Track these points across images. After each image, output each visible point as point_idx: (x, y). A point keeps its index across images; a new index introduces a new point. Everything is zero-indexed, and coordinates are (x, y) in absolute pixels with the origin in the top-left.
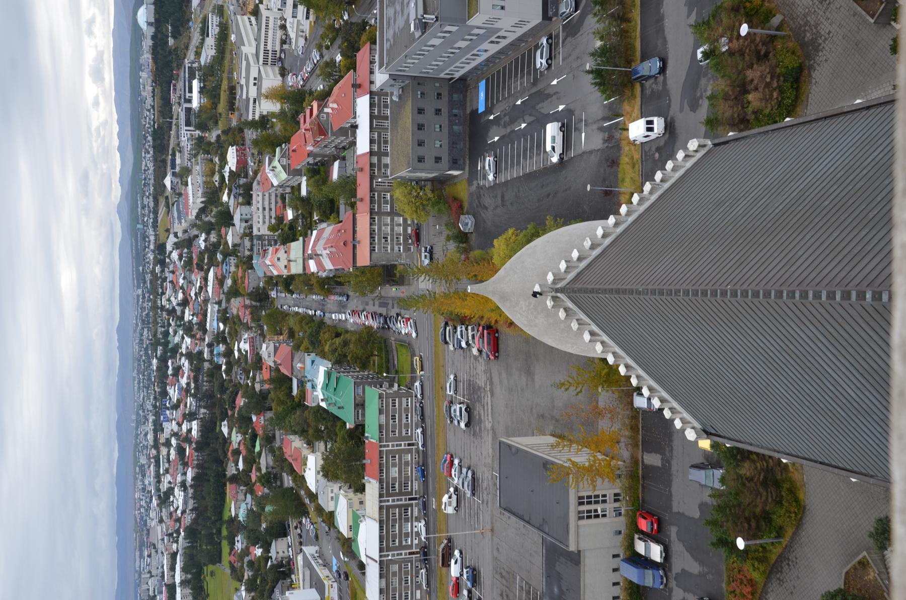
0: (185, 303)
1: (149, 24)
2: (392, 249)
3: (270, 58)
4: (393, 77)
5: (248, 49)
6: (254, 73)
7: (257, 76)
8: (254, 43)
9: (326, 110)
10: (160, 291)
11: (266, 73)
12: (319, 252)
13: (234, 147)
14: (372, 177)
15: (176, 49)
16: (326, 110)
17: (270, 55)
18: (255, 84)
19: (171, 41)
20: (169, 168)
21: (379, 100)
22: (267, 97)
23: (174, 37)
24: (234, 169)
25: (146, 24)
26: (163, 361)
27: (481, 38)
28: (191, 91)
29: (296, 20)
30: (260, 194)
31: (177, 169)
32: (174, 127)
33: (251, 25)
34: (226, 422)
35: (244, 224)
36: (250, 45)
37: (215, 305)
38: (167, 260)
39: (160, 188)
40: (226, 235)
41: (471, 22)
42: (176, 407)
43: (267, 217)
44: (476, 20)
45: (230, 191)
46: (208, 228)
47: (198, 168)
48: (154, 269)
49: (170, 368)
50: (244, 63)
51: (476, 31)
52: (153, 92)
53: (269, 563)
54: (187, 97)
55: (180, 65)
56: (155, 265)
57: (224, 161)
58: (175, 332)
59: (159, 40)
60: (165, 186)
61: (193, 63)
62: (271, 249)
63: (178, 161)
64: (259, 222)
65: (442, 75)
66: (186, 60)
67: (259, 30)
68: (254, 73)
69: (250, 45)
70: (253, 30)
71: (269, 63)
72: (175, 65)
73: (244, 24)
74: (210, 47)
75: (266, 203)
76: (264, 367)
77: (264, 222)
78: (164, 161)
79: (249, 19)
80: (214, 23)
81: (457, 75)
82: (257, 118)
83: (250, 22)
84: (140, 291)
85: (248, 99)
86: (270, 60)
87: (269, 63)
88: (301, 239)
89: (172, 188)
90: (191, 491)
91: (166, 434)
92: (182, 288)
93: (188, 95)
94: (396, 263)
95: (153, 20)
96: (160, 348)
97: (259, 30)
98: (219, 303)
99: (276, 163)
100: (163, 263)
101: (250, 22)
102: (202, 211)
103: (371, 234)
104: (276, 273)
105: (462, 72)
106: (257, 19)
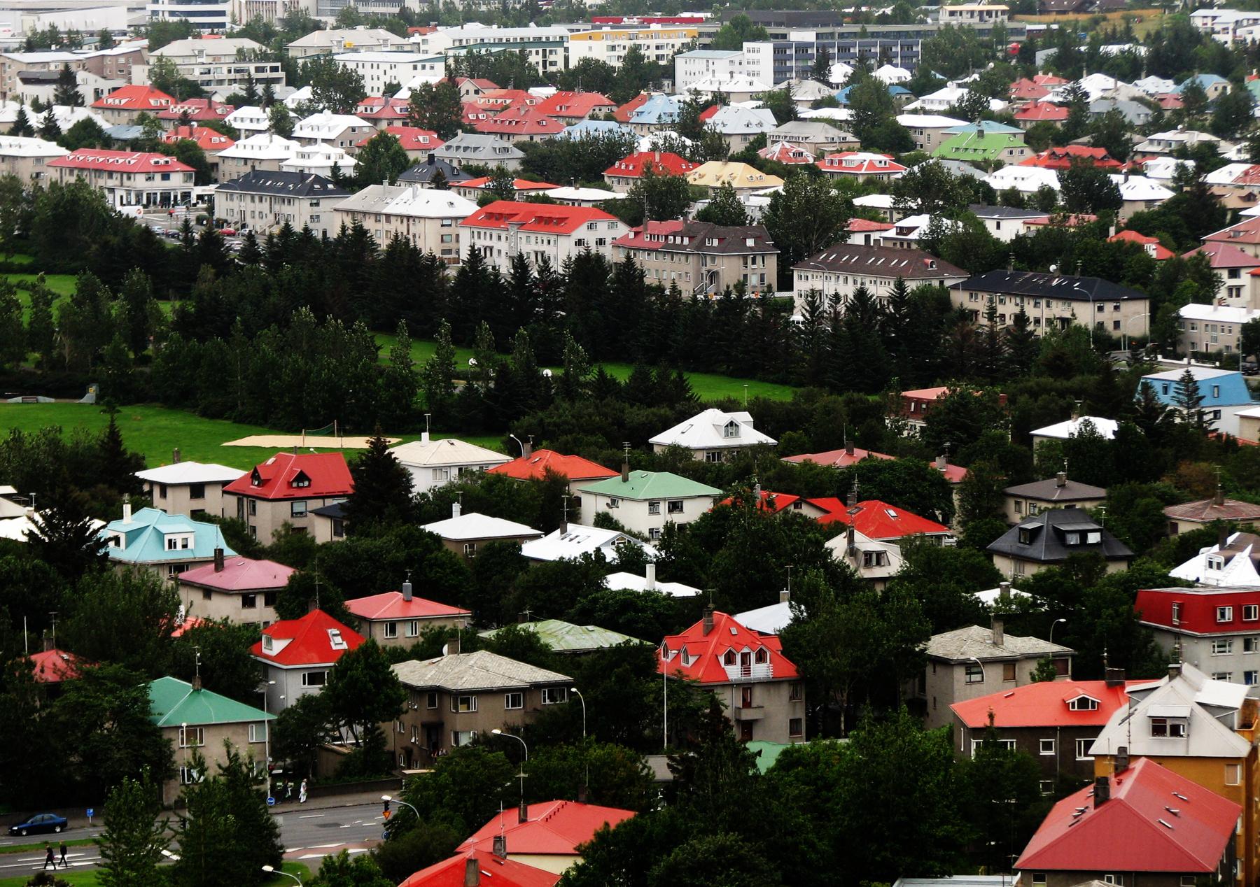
34: (750, 436)
76: (1091, 689)
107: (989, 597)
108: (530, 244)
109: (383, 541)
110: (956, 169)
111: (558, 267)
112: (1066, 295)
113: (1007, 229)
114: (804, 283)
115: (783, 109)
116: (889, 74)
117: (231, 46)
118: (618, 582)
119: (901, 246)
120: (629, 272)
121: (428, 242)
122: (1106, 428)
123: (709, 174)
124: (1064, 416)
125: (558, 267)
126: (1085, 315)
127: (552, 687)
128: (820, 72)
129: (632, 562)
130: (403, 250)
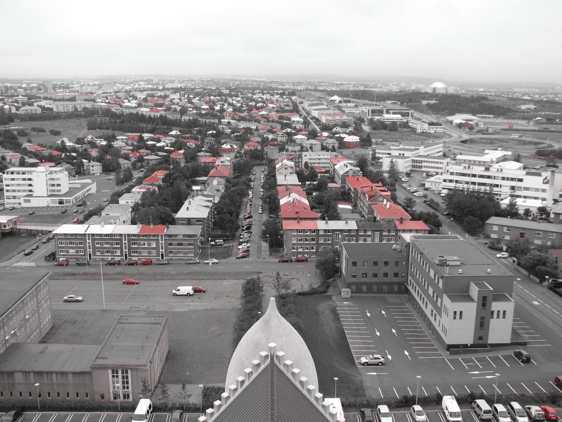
1: (434, 89)
2: (294, 244)
3: (417, 164)
4: (408, 245)
5: (422, 151)
6: (407, 154)
7: (405, 156)
8: (426, 154)
9: (385, 200)
10: (266, 92)
11: (406, 162)
12: (291, 195)
13: (359, 140)
14: (342, 231)
16: (385, 200)
17: (419, 164)
18: (400, 154)
19: (424, 102)
21: (392, 236)
22: (392, 162)
24: (345, 140)
25: (434, 87)
27: (434, 304)
28: (394, 113)
29: (442, 181)
30: (329, 157)
31: (344, 104)
32: (370, 102)
33: (437, 153)
34: (179, 133)
35: (309, 146)
36: (425, 151)
37: (255, 127)
39: (332, 93)
40: (303, 135)
41: (445, 296)
42: (190, 101)
43: (314, 161)
44: (446, 300)
46: (306, 123)
47: (345, 117)
50: (413, 148)
51: (439, 300)
53: (84, 161)
54: (390, 111)
55: (411, 108)
56: (282, 89)
57: (350, 134)
58: (238, 101)
59: (426, 96)
60: (333, 96)
61: (412, 115)
62: (293, 163)
63: (349, 104)
64: (311, 156)
65: (410, 278)
66: (413, 111)
67: (435, 158)
68: (407, 154)
69: (425, 151)
70: (434, 153)
71: (414, 164)
72: (410, 104)
73: (437, 149)
74: (422, 126)
75: (323, 161)
76: (214, 158)
77: (310, 159)
78: (348, 96)
79: (441, 151)
80: (437, 129)
81: (410, 288)
82: (377, 155)
83: (439, 152)
85: (390, 149)
86: (415, 164)
87: (414, 164)
88: (300, 183)
89: (331, 101)
90: (134, 111)
91: (172, 96)
92: (267, 106)
93: (391, 111)
94: (285, 247)
95: (438, 91)
96: (228, 92)
97: (435, 158)
98: (257, 130)
99: (350, 167)
101: (439, 152)
102: (317, 121)
103: (304, 230)
104: (277, 166)
105: (412, 291)
107: (203, 149)
108: (155, 114)
109: (142, 144)
110: (198, 106)
111: (158, 116)
112: (210, 119)
113: (204, 112)
114: (183, 118)
115: (180, 100)
116: (191, 96)
117: (124, 93)
118: (166, 148)
119: (193, 114)
120: (166, 117)
121: (145, 114)
122: (215, 132)
123: (173, 106)
124: (210, 131)
125: (158, 116)
126: (212, 121)
127: (160, 159)
128: (184, 96)
129: (167, 146)
130: (142, 114)
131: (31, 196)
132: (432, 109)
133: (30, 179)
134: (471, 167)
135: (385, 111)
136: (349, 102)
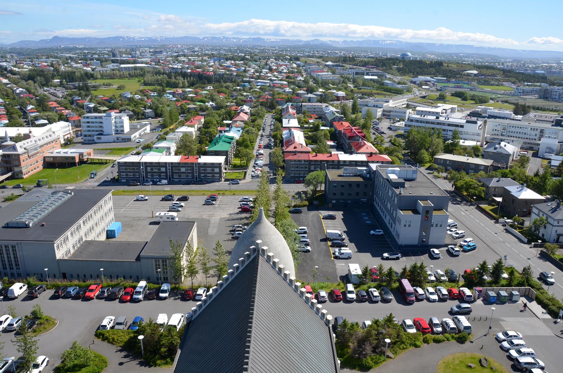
0: (271, 70)
15: (391, 69)
20: (336, 64)
23: (397, 69)
26: (243, 59)
34: (212, 88)
38: (292, 62)
40: (304, 90)
45: (324, 92)
48: (288, 55)
49: (239, 62)
52: (372, 58)
60: (327, 62)
61: (386, 77)
63: (339, 68)
72: (384, 68)
75: (318, 110)
84: (277, 48)
86: (386, 113)
87: (384, 113)
93: (370, 74)
100: (291, 60)
106: (405, 108)
131: (102, 134)
132: (401, 71)
133: (101, 123)
134: (426, 116)
135: (365, 74)
136: (339, 66)
